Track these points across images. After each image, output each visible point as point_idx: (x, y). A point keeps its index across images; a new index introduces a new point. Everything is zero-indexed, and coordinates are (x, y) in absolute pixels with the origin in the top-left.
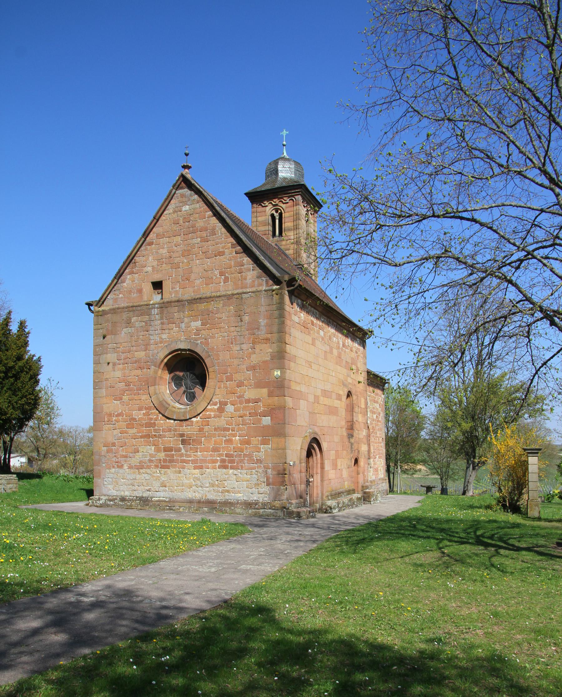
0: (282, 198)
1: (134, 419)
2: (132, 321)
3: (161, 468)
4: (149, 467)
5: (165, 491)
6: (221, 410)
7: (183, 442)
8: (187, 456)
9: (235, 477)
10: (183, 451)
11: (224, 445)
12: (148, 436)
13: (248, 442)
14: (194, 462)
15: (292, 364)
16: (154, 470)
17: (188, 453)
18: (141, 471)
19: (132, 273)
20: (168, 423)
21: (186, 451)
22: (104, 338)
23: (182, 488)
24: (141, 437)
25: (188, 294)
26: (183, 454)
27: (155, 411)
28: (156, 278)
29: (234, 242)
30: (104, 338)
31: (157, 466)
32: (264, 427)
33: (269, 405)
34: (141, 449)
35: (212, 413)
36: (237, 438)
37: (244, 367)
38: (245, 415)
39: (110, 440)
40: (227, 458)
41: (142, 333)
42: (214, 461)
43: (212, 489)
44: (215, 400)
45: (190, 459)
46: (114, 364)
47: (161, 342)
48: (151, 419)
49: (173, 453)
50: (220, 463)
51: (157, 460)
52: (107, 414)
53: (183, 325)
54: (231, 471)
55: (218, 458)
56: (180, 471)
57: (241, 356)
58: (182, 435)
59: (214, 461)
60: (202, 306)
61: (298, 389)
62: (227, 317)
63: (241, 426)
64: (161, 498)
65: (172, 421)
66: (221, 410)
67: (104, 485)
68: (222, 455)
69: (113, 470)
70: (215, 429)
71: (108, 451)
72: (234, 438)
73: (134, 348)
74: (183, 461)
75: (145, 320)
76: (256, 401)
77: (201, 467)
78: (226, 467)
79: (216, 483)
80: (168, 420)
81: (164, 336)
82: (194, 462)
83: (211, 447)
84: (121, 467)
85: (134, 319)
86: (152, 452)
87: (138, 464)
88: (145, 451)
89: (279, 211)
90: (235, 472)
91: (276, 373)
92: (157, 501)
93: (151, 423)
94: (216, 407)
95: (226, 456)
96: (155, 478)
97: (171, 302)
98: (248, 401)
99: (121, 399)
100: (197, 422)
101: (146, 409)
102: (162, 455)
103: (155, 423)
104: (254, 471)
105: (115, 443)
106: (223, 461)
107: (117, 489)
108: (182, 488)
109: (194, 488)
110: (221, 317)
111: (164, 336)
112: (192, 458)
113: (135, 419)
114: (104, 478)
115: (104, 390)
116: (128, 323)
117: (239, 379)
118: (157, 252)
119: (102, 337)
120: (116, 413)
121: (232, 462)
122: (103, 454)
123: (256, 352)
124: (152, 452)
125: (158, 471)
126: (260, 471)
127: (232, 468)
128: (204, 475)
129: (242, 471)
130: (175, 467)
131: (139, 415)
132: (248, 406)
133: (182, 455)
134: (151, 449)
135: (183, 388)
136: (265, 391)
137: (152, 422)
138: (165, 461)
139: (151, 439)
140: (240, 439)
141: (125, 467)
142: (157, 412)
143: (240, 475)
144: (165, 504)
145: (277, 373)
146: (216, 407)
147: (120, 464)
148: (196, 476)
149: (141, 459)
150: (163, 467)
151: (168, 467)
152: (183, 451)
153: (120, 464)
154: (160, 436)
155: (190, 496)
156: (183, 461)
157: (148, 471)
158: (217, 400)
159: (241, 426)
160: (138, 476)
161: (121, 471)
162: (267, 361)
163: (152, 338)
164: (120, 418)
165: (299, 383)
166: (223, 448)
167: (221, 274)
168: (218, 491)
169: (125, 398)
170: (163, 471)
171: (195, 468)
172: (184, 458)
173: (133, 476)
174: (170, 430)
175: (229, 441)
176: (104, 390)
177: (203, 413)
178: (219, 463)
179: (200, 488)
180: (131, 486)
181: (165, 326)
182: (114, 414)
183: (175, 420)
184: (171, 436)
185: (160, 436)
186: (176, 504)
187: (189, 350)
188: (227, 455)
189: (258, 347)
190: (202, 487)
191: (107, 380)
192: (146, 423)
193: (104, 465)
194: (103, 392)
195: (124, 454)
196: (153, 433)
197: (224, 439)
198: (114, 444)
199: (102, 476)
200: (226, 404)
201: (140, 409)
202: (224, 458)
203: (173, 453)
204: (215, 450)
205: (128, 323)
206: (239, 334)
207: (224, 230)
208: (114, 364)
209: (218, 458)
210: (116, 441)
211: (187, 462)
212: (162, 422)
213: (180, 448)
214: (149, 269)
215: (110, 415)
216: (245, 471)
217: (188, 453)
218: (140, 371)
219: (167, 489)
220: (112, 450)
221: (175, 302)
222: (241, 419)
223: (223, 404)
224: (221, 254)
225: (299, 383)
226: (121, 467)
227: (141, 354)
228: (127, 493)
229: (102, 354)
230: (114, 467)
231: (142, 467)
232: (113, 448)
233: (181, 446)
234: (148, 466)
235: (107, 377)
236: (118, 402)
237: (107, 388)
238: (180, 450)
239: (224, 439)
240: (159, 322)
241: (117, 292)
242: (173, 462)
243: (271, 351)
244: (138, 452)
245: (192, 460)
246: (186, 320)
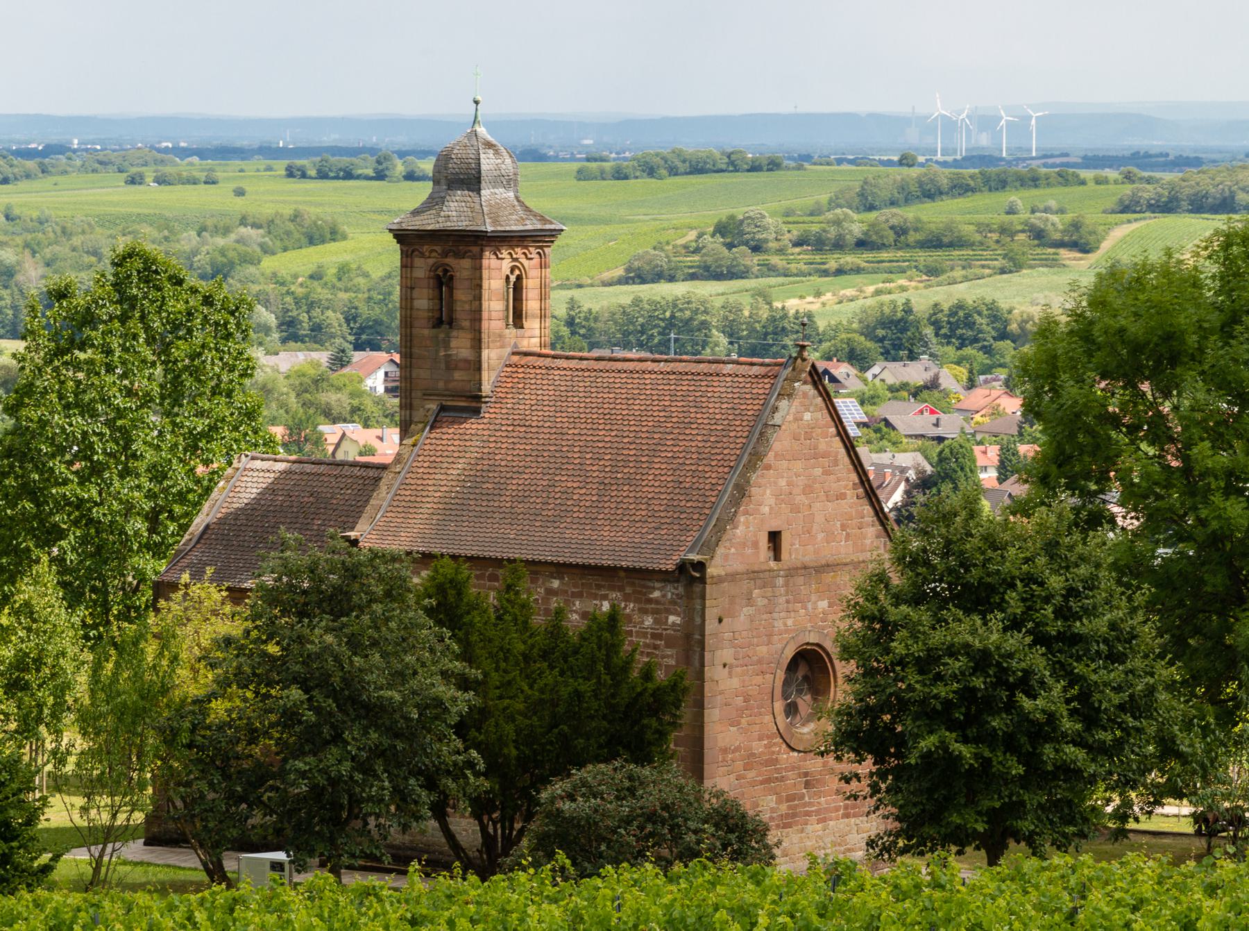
0: (526, 247)
7: (807, 785)
14: (818, 812)
22: (720, 621)
24: (762, 783)
25: (809, 559)
27: (779, 740)
29: (857, 481)
30: (720, 621)
42: (837, 809)
46: (731, 667)
47: (787, 631)
48: (773, 753)
58: (806, 774)
59: (837, 809)
65: (796, 754)
78: (847, 816)
86: (773, 805)
89: (517, 272)
90: (858, 822)
99: (739, 723)
101: (768, 737)
102: (784, 808)
111: (790, 622)
116: (749, 600)
130: (796, 823)
131: (758, 747)
133: (805, 805)
154: (782, 779)
164: (737, 754)
167: (843, 527)
174: (793, 768)
183: (799, 752)
185: (782, 779)
191: (722, 693)
201: (760, 739)
205: (749, 600)
207: (847, 460)
211: (808, 814)
214: (766, 509)
215: (725, 751)
224: (842, 496)
227: (763, 650)
229: (717, 649)
241: (727, 544)
246: (813, 598)
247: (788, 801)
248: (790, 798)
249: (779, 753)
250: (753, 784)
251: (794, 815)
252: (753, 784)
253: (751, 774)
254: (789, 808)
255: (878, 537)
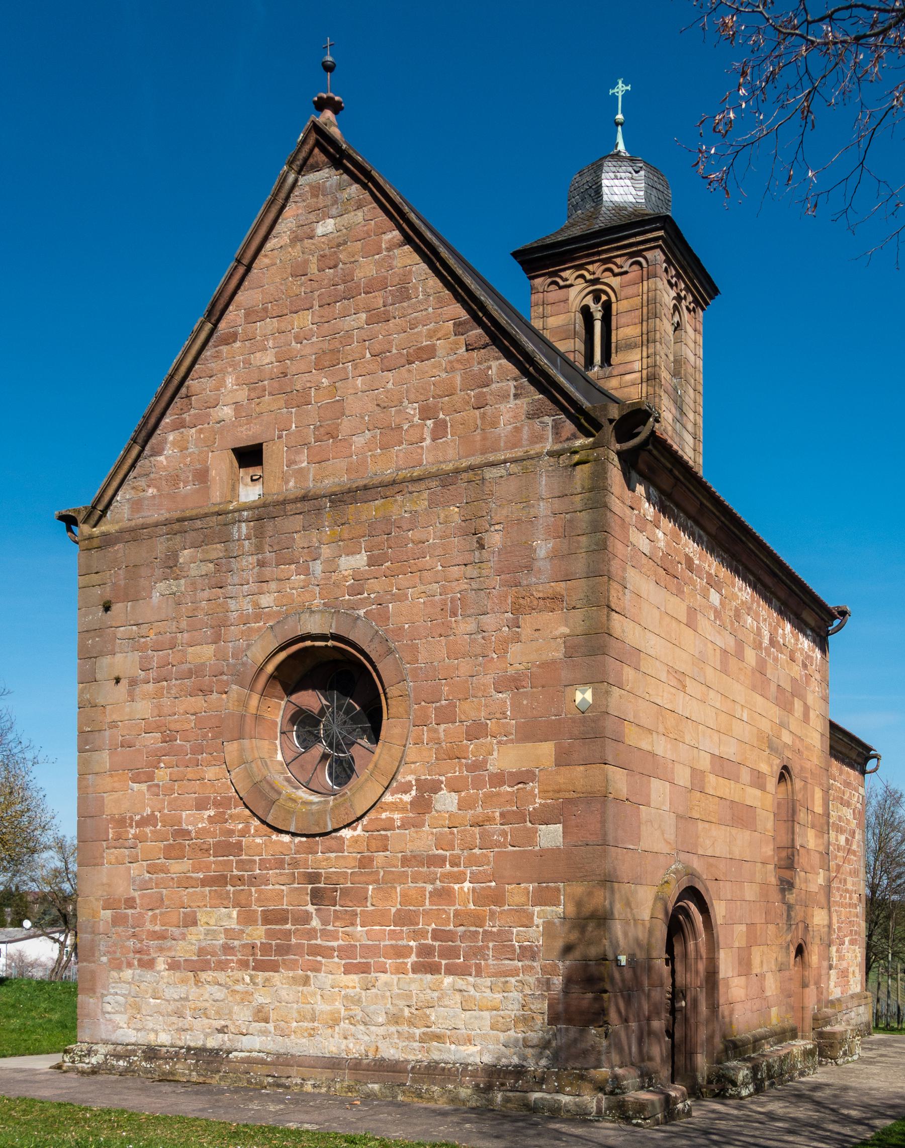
1: (186, 833)
2: (181, 560)
3: (254, 969)
4: (222, 966)
5: (265, 1033)
6: (422, 805)
7: (317, 897)
8: (325, 934)
9: (458, 997)
10: (315, 923)
11: (428, 906)
12: (221, 880)
13: (497, 898)
14: (346, 952)
15: (629, 673)
16: (238, 974)
17: (330, 928)
18: (203, 976)
19: (180, 425)
20: (276, 842)
21: (325, 922)
22: (107, 608)
23: (311, 1025)
24: (204, 883)
26: (314, 930)
27: (240, 810)
28: (246, 436)
31: (244, 965)
32: (543, 853)
33: (559, 791)
34: (201, 917)
35: (397, 816)
36: (467, 885)
37: (489, 679)
38: (490, 819)
39: (122, 889)
40: (437, 944)
41: (206, 594)
43: (393, 1029)
44: (407, 777)
45: (335, 944)
46: (133, 682)
47: (258, 617)
48: (231, 832)
49: (288, 926)
50: (418, 956)
51: (244, 946)
52: (113, 818)
53: (317, 567)
54: (448, 980)
55: (412, 943)
56: (308, 977)
57: (478, 650)
58: (313, 878)
60: (371, 510)
61: (645, 745)
62: (441, 538)
63: (477, 851)
64: (255, 1054)
65: (286, 838)
66: (422, 805)
67: (104, 1013)
68: (422, 934)
69: (128, 974)
70: (405, 861)
71: (117, 921)
72: (456, 887)
73: (186, 635)
74: (316, 951)
75: (214, 555)
76: (522, 778)
77: (364, 969)
78: (433, 969)
79: (407, 1012)
80: (274, 837)
81: (266, 600)
82: (346, 952)
83: (393, 910)
84: (148, 965)
85: (185, 555)
86: (233, 925)
87: (195, 958)
88: (212, 922)
90: (460, 982)
91: (579, 697)
92: (244, 1061)
93: (230, 844)
94: (407, 798)
95: (434, 938)
96: (238, 997)
97: (284, 502)
98: (499, 779)
99: (150, 778)
100: (355, 840)
101: (217, 804)
102: (258, 933)
103: (240, 843)
104: (513, 980)
105: (133, 899)
106: (426, 951)
107: (139, 1026)
108: (311, 1025)
109: (346, 1025)
110: (423, 537)
111: (266, 600)
112: (341, 942)
113: (188, 832)
114: (103, 995)
115: (105, 755)
116: (171, 566)
117: (473, 714)
118: (247, 362)
119: (101, 608)
120: (138, 817)
121: (451, 953)
122: (102, 927)
123: (523, 638)
124: (233, 925)
125: (247, 979)
126: (532, 980)
127: (450, 971)
128: (374, 990)
129: (479, 980)
130: (292, 966)
132: (498, 794)
133: (312, 934)
134: (229, 917)
135: (321, 748)
136: (547, 749)
137: (233, 840)
138: (266, 949)
139: (229, 888)
140: (474, 889)
141: (161, 964)
142: (247, 812)
143: (472, 991)
144: (265, 1070)
145: (584, 696)
146: (407, 798)
147: (146, 957)
148: (351, 992)
149: (203, 944)
150: (260, 966)
151: (274, 967)
152: (315, 923)
153: (146, 957)
154: (253, 881)
155: (334, 1049)
156: (316, 951)
157: (221, 976)
158: (411, 778)
159: (477, 851)
160: (194, 992)
161: (149, 976)
162: (554, 662)
163: (233, 607)
164: (148, 830)
165: (650, 731)
166: (426, 913)
168: (411, 1037)
169: (162, 775)
170: (261, 976)
171: (348, 970)
172: (319, 942)
173: (182, 991)
174: (280, 864)
175: (443, 895)
176: (105, 755)
177: (372, 815)
178: (413, 958)
179: (362, 1027)
180: (174, 1019)
181: (268, 572)
182: (131, 818)
183: (294, 835)
184: (283, 879)
185: (253, 881)
186: (293, 1071)
187: (335, 637)
188: (436, 935)
189: (528, 622)
190: (365, 1024)
191: (113, 725)
192: (217, 845)
193: (104, 959)
194: (104, 759)
195: (157, 928)
196: (235, 872)
197: (429, 887)
198: (130, 903)
199: (100, 990)
200: (435, 788)
201: (201, 805)
202: (430, 942)
203: (288, 926)
204: (405, 918)
205: (171, 566)
206: (475, 586)
208: (133, 682)
209: (412, 943)
210: (136, 894)
211: (326, 952)
212: (258, 840)
213: (307, 911)
214: (227, 412)
215: (122, 822)
216: (488, 981)
217: (330, 928)
218: (200, 698)
219: (270, 1026)
220: (126, 916)
221: (296, 500)
222: (477, 830)
223: (426, 789)
225: (650, 731)
226: (148, 965)
227: (206, 652)
228: (164, 1038)
229: (102, 654)
230: (130, 965)
231: (205, 966)
232: (130, 911)
233: (311, 908)
234: (220, 962)
235: (115, 717)
236: (144, 787)
237: (113, 749)
238: (306, 918)
239: (429, 887)
240: (253, 559)
241: (142, 482)
242: (287, 953)
243: (565, 630)
244: (195, 923)
245: (340, 949)
246: (326, 551)
247: (266, 921)
248: (270, 918)
249: (244, 833)
250: (185, 882)
251: (283, 950)
252: (185, 882)
253: (178, 867)
254: (270, 934)
255: (531, 416)
